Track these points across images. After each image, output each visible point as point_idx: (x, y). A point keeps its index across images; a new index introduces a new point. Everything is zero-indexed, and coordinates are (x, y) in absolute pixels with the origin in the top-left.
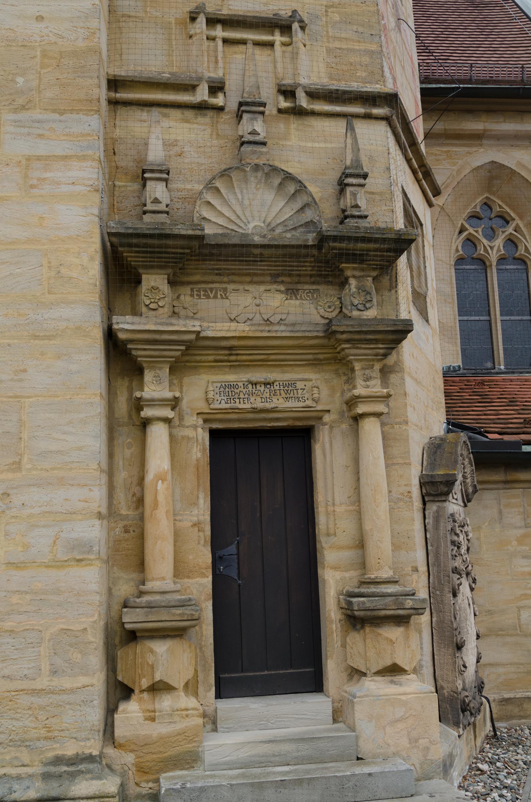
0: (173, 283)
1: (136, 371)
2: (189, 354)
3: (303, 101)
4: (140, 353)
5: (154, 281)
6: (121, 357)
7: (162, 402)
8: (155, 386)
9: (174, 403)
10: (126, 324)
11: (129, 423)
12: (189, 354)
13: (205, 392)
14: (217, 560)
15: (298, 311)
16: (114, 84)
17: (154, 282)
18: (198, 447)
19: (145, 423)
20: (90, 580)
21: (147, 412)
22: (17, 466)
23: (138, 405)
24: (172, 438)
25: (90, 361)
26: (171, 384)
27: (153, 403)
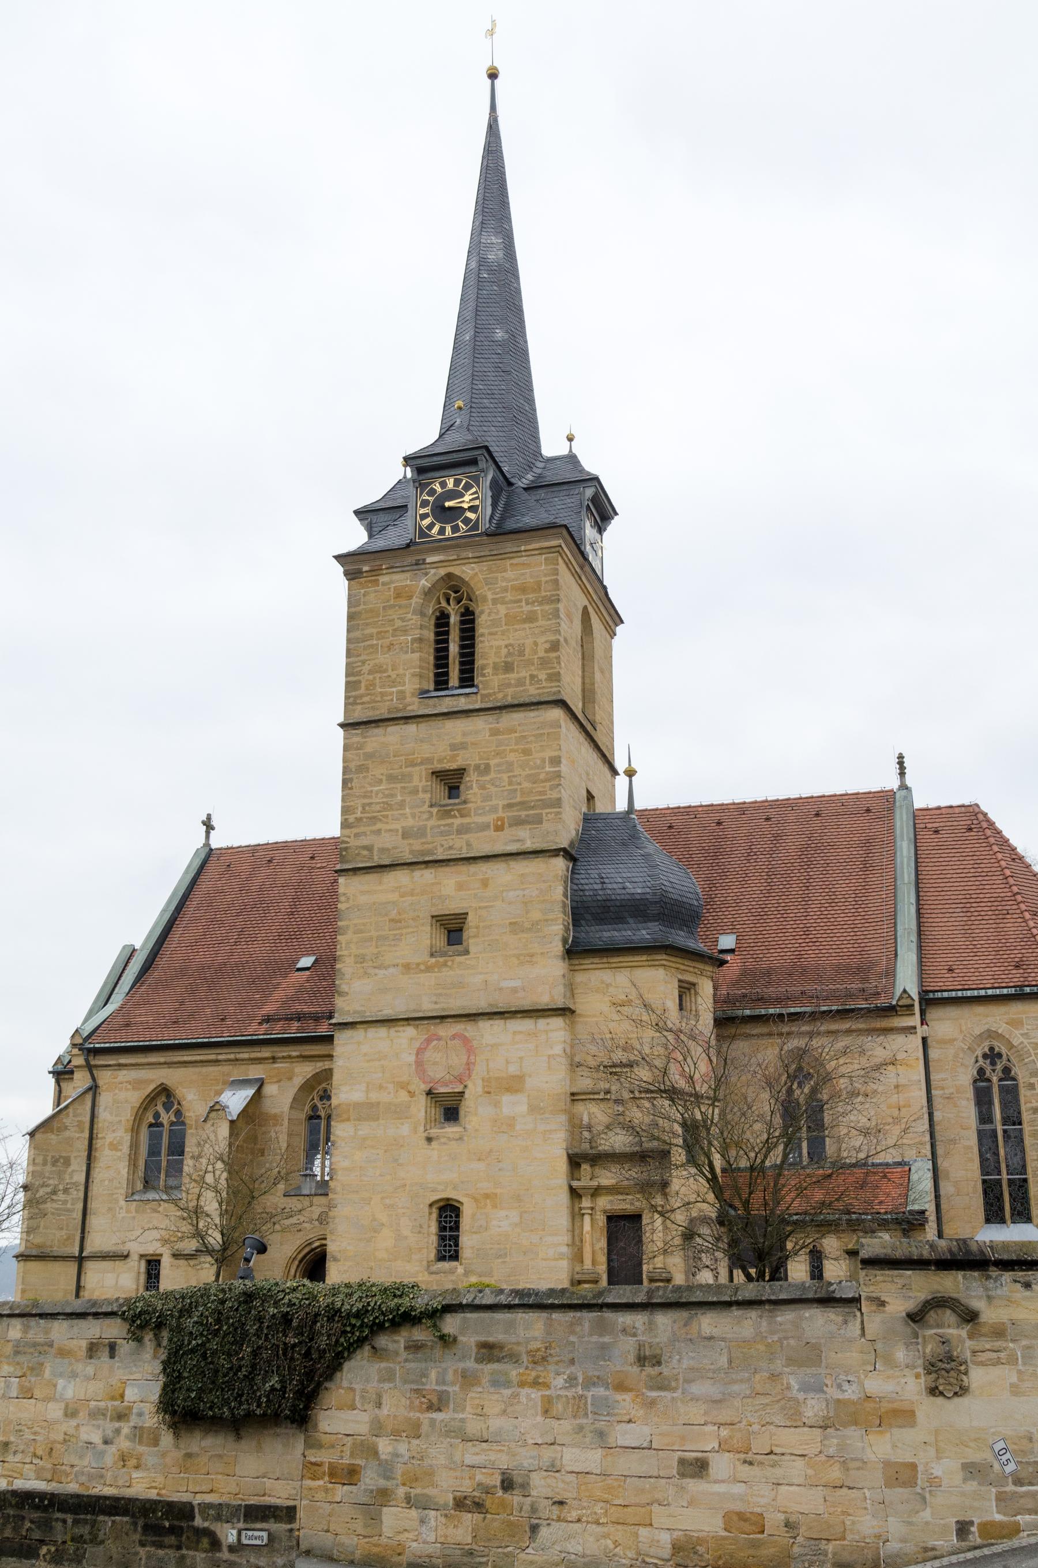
0: (591, 1166)
1: (580, 1197)
2: (596, 1192)
3: (637, 1095)
4: (580, 1192)
5: (585, 1167)
6: (575, 1194)
7: (588, 1208)
8: (586, 1203)
9: (592, 1209)
10: (575, 1184)
11: (576, 1215)
12: (596, 1192)
13: (604, 1202)
14: (609, 1261)
15: (634, 1173)
16: (573, 1094)
17: (585, 1167)
18: (601, 1220)
19: (583, 1214)
20: (564, 1264)
21: (583, 1211)
22: (544, 1230)
23: (581, 1209)
24: (592, 1219)
25: (564, 1197)
26: (592, 1201)
27: (584, 1208)
